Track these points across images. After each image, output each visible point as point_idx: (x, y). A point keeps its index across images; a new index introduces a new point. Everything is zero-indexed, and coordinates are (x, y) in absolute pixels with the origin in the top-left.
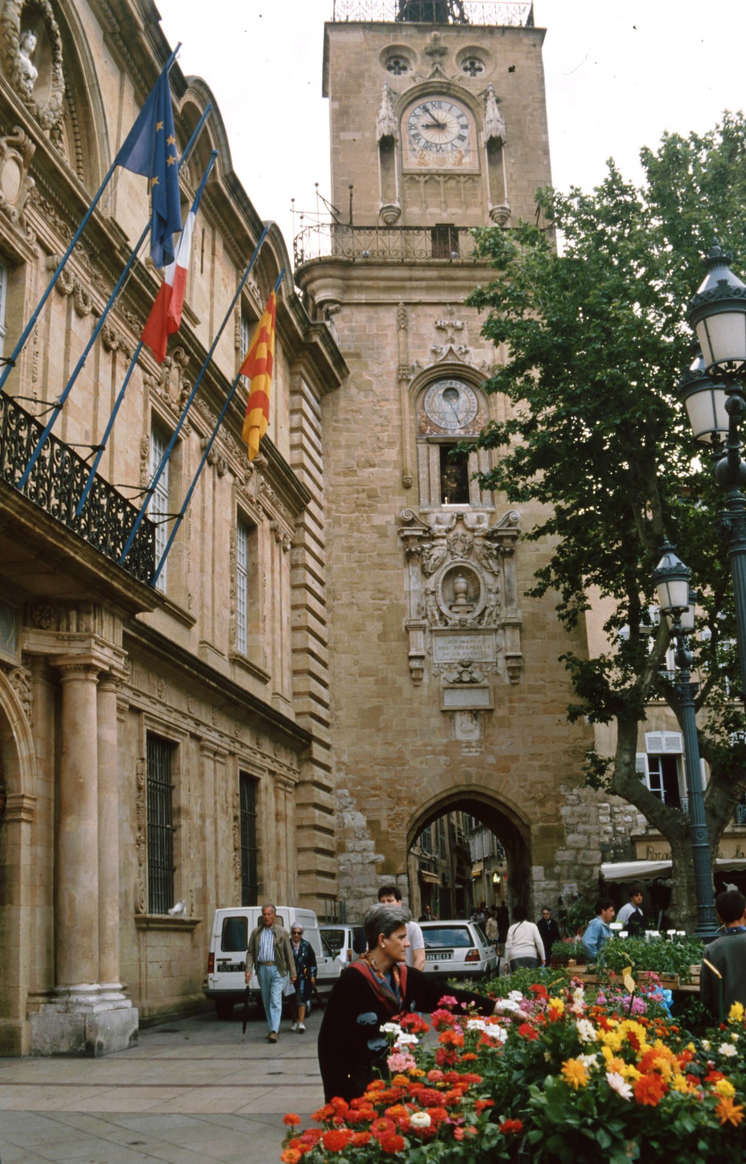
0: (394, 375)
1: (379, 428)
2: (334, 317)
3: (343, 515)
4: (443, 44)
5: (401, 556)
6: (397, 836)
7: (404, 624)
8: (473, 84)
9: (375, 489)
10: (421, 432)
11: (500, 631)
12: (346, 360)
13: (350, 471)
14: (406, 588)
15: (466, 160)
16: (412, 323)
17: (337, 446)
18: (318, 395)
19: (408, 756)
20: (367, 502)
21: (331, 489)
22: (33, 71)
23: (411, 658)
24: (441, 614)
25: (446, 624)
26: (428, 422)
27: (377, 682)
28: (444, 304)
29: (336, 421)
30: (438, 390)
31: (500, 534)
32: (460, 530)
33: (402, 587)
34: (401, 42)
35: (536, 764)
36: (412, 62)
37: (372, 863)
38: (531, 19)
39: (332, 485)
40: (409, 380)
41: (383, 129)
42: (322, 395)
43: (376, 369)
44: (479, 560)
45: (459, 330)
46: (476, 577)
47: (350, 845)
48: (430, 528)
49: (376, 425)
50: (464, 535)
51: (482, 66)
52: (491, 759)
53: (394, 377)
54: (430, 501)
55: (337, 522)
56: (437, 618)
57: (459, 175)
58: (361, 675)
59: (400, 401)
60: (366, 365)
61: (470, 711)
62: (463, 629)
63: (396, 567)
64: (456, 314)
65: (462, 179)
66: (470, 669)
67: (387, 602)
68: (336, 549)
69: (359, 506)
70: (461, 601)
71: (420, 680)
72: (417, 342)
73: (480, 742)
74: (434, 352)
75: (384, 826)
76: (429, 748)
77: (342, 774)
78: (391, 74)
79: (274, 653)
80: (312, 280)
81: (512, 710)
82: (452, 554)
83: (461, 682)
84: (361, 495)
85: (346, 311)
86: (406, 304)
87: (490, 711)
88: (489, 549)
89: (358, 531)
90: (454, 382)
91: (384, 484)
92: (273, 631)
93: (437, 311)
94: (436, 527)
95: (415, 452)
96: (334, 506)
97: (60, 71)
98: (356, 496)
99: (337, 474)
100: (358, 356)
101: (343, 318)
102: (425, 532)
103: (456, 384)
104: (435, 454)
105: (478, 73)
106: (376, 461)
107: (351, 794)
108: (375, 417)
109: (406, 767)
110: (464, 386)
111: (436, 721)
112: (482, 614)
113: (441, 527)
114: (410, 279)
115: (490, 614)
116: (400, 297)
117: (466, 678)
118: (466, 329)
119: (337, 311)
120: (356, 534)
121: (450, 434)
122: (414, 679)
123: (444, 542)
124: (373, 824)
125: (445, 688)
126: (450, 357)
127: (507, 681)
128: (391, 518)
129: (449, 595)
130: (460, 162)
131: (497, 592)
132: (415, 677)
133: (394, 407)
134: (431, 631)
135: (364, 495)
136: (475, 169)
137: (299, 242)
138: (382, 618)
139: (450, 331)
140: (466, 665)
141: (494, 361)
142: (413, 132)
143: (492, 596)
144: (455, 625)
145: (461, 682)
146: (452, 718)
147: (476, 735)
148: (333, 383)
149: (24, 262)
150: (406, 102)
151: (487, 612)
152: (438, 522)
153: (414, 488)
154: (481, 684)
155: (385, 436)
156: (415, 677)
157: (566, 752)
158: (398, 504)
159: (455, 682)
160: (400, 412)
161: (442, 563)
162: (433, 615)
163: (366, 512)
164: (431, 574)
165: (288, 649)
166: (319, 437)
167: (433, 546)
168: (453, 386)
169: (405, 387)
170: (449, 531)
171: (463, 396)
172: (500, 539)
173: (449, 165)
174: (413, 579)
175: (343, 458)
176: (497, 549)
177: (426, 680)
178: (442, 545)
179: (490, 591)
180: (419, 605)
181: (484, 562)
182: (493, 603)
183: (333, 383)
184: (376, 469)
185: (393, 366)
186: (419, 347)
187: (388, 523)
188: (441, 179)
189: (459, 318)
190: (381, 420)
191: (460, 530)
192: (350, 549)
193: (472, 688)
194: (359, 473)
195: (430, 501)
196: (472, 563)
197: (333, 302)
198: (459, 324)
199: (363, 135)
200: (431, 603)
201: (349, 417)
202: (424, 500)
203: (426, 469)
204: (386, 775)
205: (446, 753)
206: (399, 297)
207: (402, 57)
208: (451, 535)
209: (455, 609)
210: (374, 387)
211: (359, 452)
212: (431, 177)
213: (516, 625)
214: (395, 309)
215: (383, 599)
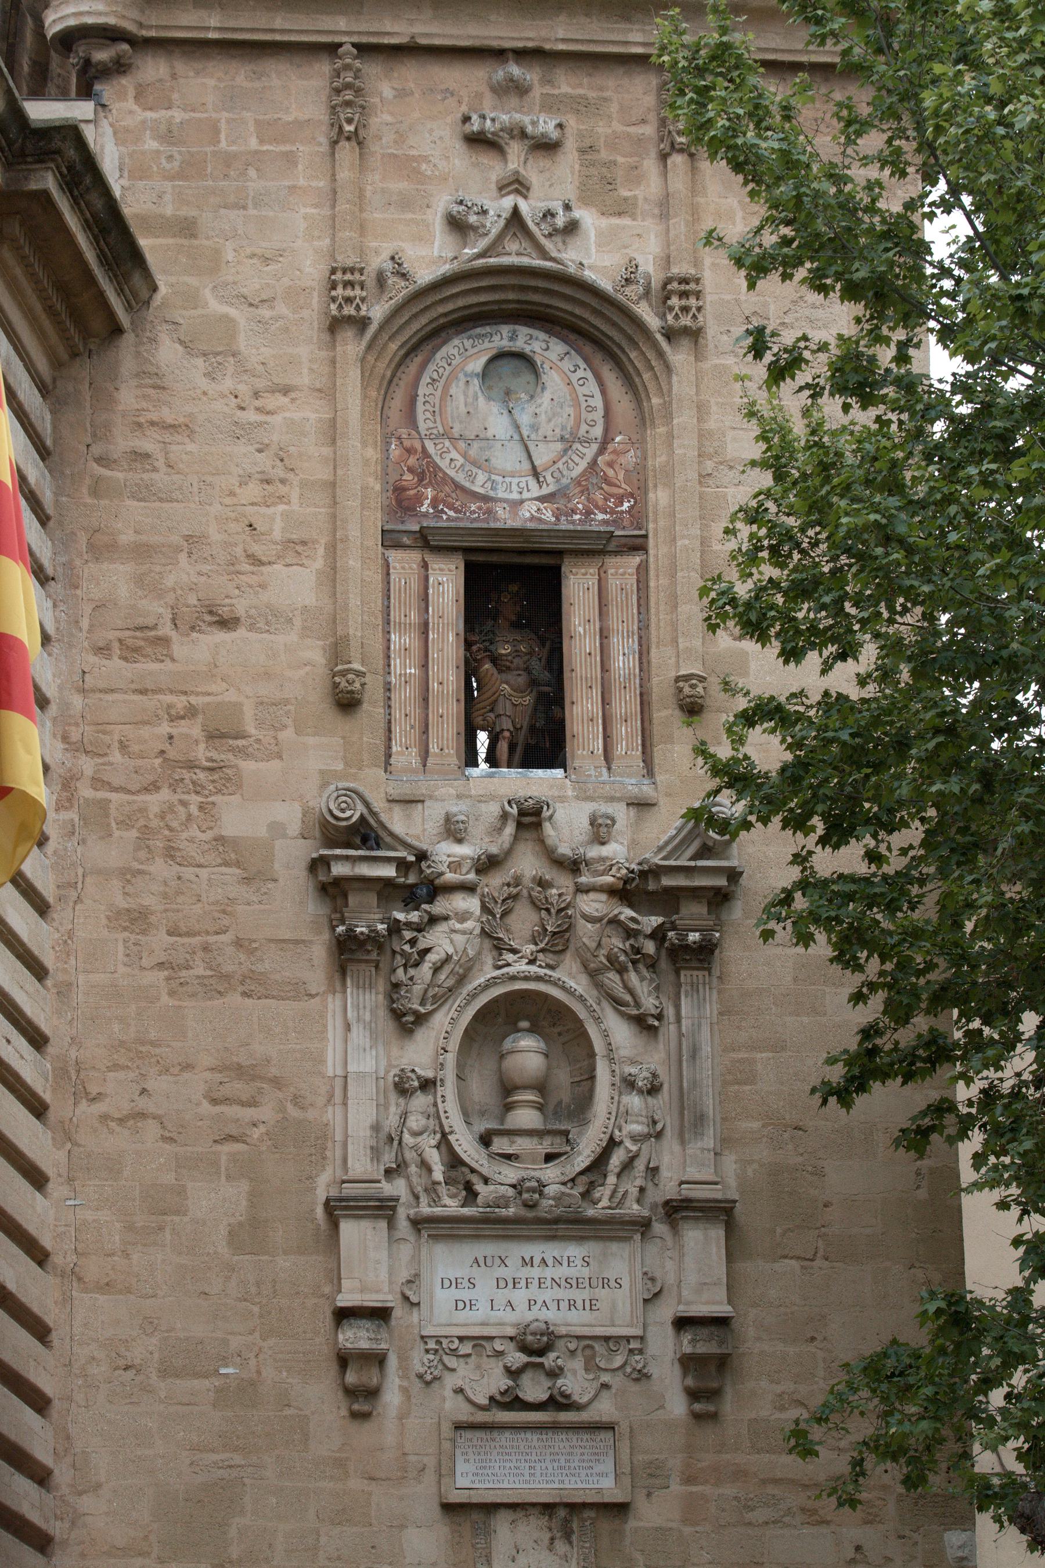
0: (316, 301)
1: (253, 490)
2: (105, 89)
3: (114, 796)
5: (319, 951)
7: (321, 1195)
9: (238, 706)
10: (402, 502)
11: (659, 1228)
12: (144, 243)
13: (144, 642)
14: (332, 1066)
16: (381, 120)
17: (102, 548)
18: (42, 365)
20: (201, 753)
21: (77, 702)
23: (343, 1315)
24: (454, 1162)
26: (428, 472)
28: (499, 54)
29: (100, 460)
30: (467, 355)
31: (667, 881)
32: (527, 864)
33: (321, 1061)
39: (83, 691)
40: (362, 323)
42: (57, 364)
43: (253, 280)
44: (594, 975)
45: (546, 146)
46: (584, 1035)
48: (422, 856)
49: (244, 480)
50: (542, 883)
53: (313, 311)
54: (425, 754)
55: (96, 817)
56: (438, 1175)
58: (165, 1373)
59: (329, 393)
60: (214, 264)
61: (548, 1508)
62: (532, 1220)
63: (298, 991)
64: (537, 92)
66: (549, 1360)
67: (266, 1113)
69: (176, 768)
70: (526, 1117)
71: (372, 1393)
72: (399, 185)
74: (457, 225)
82: (499, 947)
83: (517, 1403)
84: (183, 728)
85: (153, 69)
86: (364, 50)
87: (620, 1509)
88: (630, 934)
89: (170, 853)
90: (523, 331)
93: (468, 81)
95: (376, 578)
96: (87, 765)
98: (165, 728)
99: (102, 650)
100: (187, 228)
102: (402, 865)
104: (447, 582)
106: (241, 607)
108: (242, 449)
110: (558, 347)
113: (464, 850)
115: (628, 1165)
116: (342, 23)
117: (534, 1390)
118: (570, 145)
119: (120, 67)
120: (160, 867)
121: (505, 518)
122: (351, 1393)
123: (471, 904)
125: (459, 1427)
126: (512, 246)
127: (677, 1406)
128: (290, 815)
129: (482, 1089)
131: (653, 1090)
133: (310, 413)
134: (418, 1223)
135: (194, 729)
139: (515, 150)
140: (537, 1345)
141: (667, 261)
143: (634, 1101)
144: (502, 1202)
145: (517, 1403)
146: (488, 1533)
148: (97, 324)
151: (616, 1160)
152: (453, 831)
153: (372, 709)
154: (584, 1416)
155: (275, 522)
160: (332, 433)
161: (461, 980)
162: (425, 1166)
163: (198, 788)
164: (421, 1019)
166: (44, 520)
167: (434, 920)
168: (520, 344)
169: (351, 346)
170: (488, 864)
171: (553, 379)
172: (669, 900)
174: (359, 1036)
175: (124, 592)
176: (658, 935)
177: (392, 1397)
178: (463, 917)
179: (630, 1083)
180: (376, 1128)
181: (612, 979)
182: (637, 1128)
183: (97, 324)
184: (241, 632)
185: (312, 270)
186: (405, 203)
187: (277, 829)
189: (550, 105)
190: (265, 462)
191: (527, 864)
192: (136, 920)
193: (555, 1427)
194: (180, 648)
195: (425, 754)
196: (569, 981)
197: (109, 35)
198: (546, 125)
200: (415, 1122)
201: (147, 445)
202: (405, 756)
206: (341, 26)
208: (494, 883)
209: (500, 1145)
210: (242, 343)
211: (182, 573)
213: (720, 1212)
214: (323, 67)
215: (252, 1103)
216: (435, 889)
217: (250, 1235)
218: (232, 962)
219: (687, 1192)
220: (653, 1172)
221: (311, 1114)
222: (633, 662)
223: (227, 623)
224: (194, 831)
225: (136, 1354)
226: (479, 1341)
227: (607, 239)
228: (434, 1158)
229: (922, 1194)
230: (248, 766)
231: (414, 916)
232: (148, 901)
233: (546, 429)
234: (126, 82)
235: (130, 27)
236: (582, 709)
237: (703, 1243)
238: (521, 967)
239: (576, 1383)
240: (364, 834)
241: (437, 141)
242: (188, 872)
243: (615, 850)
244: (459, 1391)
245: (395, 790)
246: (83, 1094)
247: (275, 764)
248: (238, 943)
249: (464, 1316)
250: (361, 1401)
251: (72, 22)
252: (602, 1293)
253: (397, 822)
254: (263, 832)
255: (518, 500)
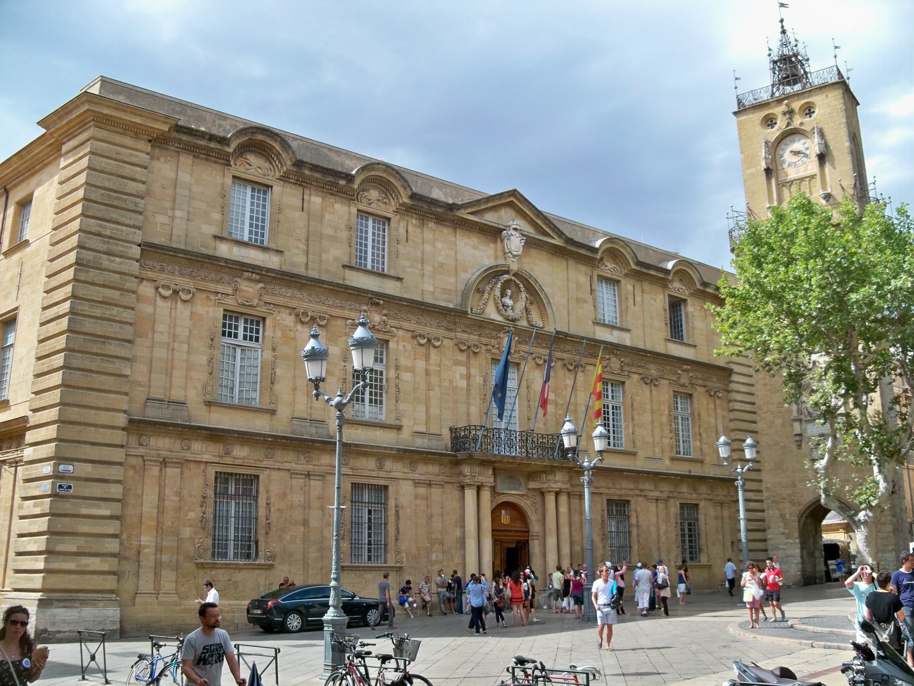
6: (793, 521)
15: (809, 167)
34: (770, 111)
37: (783, 534)
47: (772, 526)
68: (759, 386)
75: (788, 516)
107: (773, 502)
124: (782, 516)
130: (806, 170)
177: (803, 445)
204: (788, 492)
217: (783, 426)
246: (760, 409)
250: (799, 446)
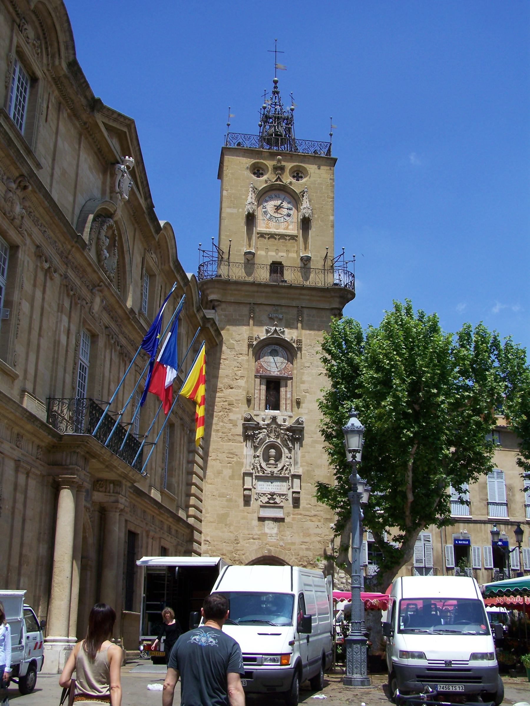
0: (247, 341)
1: (236, 369)
4: (283, 163)
8: (297, 186)
10: (258, 371)
14: (245, 453)
15: (291, 227)
19: (241, 540)
20: (227, 407)
22: (108, 255)
23: (245, 489)
24: (261, 467)
25: (264, 473)
27: (227, 501)
29: (215, 364)
30: (268, 349)
31: (294, 428)
33: (243, 452)
35: (303, 547)
36: (266, 171)
38: (329, 151)
41: (249, 208)
43: (238, 338)
51: (303, 176)
52: (281, 543)
54: (260, 408)
56: (259, 469)
57: (286, 235)
58: (219, 496)
65: (288, 238)
67: (234, 459)
73: (277, 534)
76: (251, 536)
77: (207, 546)
78: (254, 177)
79: (178, 486)
80: (208, 289)
81: (293, 519)
85: (224, 306)
89: (222, 421)
91: (237, 398)
92: (179, 476)
93: (268, 308)
94: (261, 423)
97: (116, 250)
98: (222, 403)
101: (222, 309)
103: (277, 348)
105: (300, 179)
109: (239, 545)
110: (281, 349)
111: (255, 522)
112: (282, 469)
114: (257, 292)
115: (286, 470)
116: (251, 300)
117: (271, 501)
119: (219, 305)
120: (221, 424)
121: (273, 374)
125: (261, 506)
130: (287, 228)
131: (291, 458)
132: (247, 501)
134: (256, 476)
136: (295, 232)
137: (202, 268)
138: (231, 467)
140: (272, 494)
142: (264, 210)
144: (268, 474)
147: (275, 531)
148: (214, 344)
149: (98, 335)
150: (262, 196)
151: (285, 468)
155: (239, 373)
156: (247, 501)
157: (319, 542)
158: (244, 409)
159: (266, 503)
163: (227, 412)
165: (184, 483)
167: (260, 433)
168: (276, 348)
170: (268, 425)
171: (280, 354)
173: (282, 231)
176: (292, 436)
178: (264, 432)
180: (250, 462)
184: (233, 390)
185: (246, 337)
187: (238, 419)
188: (277, 237)
195: (260, 408)
198: (281, 316)
199: (238, 211)
200: (256, 462)
203: (258, 391)
205: (259, 539)
207: (261, 168)
210: (235, 347)
212: (272, 236)
213: (299, 477)
214: (249, 306)
216: (261, 428)
217: (232, 477)
218: (231, 437)
219: (295, 473)
220: (290, 470)
221: (241, 460)
222: (290, 396)
223: (231, 388)
224: (226, 418)
225: (215, 494)
226: (264, 494)
227: (289, 333)
228: (259, 467)
229: (329, 475)
230: (234, 409)
231: (257, 432)
232: (219, 428)
233: (279, 361)
234: (220, 307)
235: (220, 299)
236: (282, 402)
237: (296, 481)
238: (272, 440)
239: (278, 500)
240: (251, 419)
241: (264, 318)
242: (225, 424)
243: (286, 423)
244: (261, 501)
245: (255, 413)
247: (238, 409)
248: (232, 435)
249: (262, 490)
251: (212, 299)
252: (282, 487)
253: (255, 418)
254: (236, 419)
255: (274, 372)
